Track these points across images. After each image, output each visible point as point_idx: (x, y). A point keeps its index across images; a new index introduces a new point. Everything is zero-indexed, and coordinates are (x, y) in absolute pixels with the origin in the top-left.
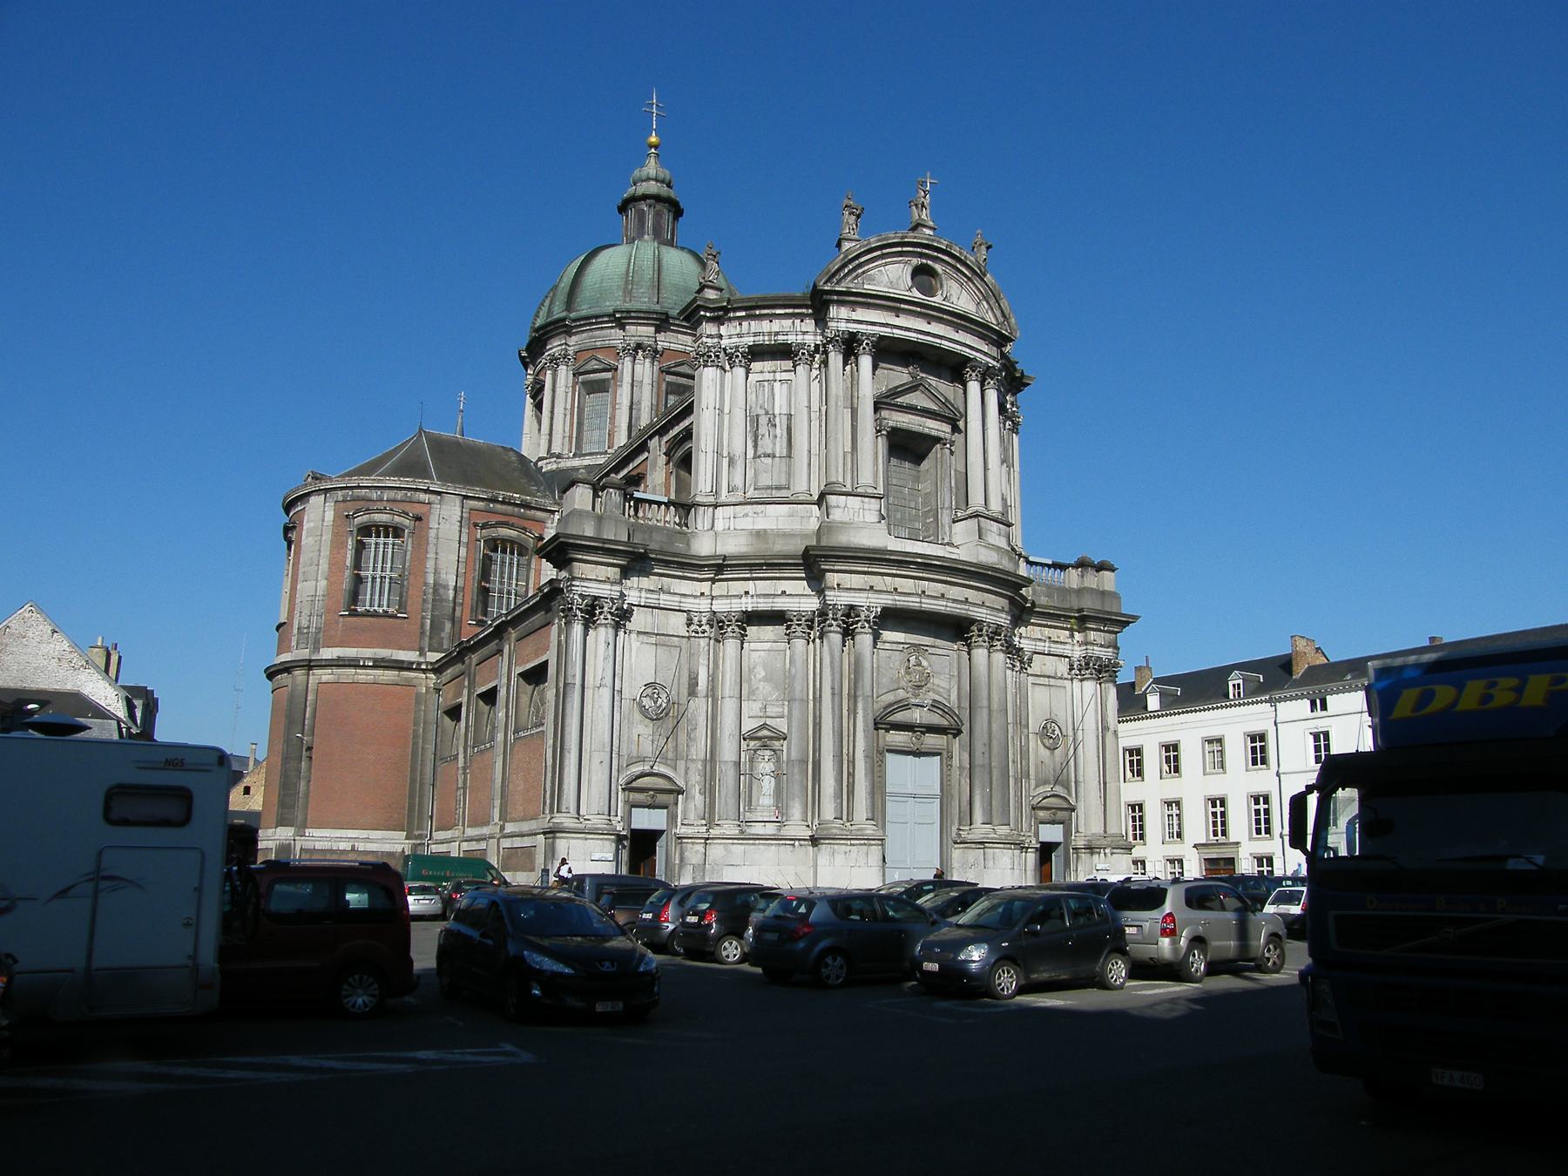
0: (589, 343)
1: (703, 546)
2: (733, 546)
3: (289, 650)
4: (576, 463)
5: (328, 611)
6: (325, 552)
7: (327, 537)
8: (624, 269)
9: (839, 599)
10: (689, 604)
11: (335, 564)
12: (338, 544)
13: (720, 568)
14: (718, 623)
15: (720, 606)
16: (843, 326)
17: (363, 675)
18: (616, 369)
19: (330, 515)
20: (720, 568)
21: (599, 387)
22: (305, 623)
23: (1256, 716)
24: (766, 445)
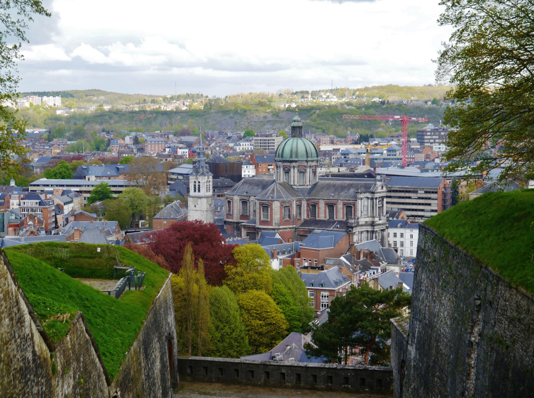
0: (300, 164)
1: (360, 223)
2: (363, 223)
3: (272, 225)
4: (300, 187)
5: (280, 220)
6: (279, 211)
7: (279, 208)
8: (305, 149)
9: (375, 230)
10: (359, 230)
11: (281, 213)
12: (281, 210)
13: (362, 225)
14: (362, 232)
15: (362, 230)
16: (376, 196)
17: (287, 230)
18: (305, 170)
19: (279, 205)
20: (362, 225)
21: (304, 173)
22: (276, 222)
23: (402, 230)
24: (364, 209)
